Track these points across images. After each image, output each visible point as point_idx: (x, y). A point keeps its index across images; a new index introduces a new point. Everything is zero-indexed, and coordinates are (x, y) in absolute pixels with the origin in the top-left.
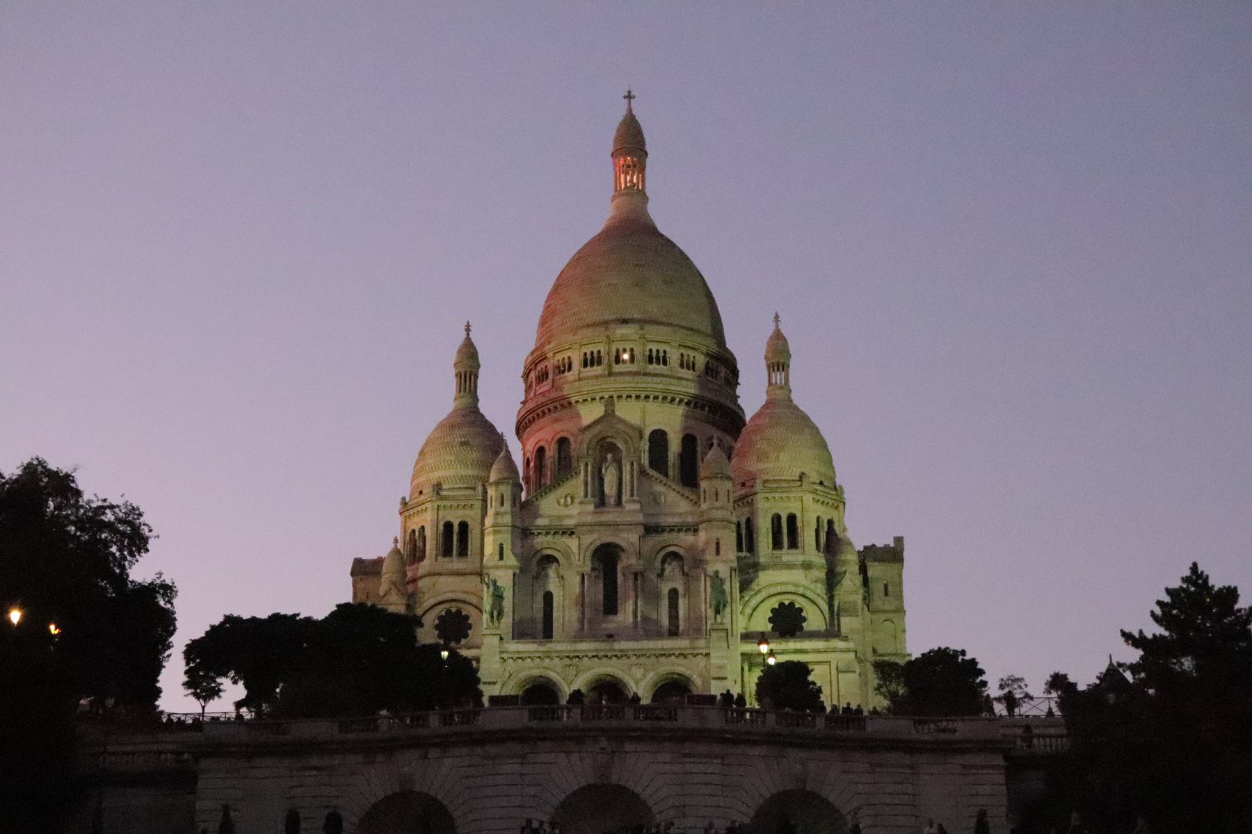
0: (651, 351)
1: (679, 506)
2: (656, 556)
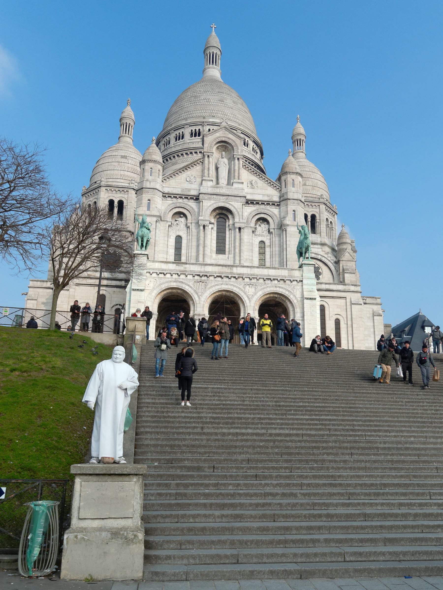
1: (267, 190)
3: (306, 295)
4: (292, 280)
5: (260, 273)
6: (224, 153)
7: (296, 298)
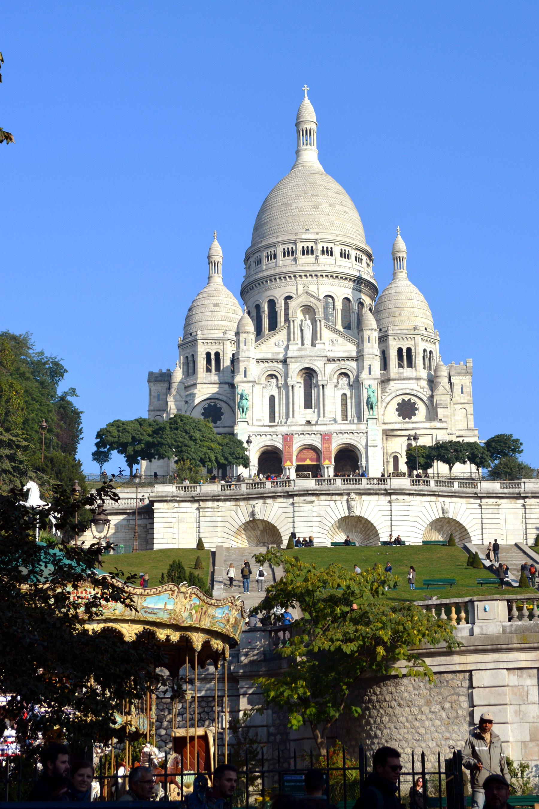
0: (323, 247)
6: (307, 316)
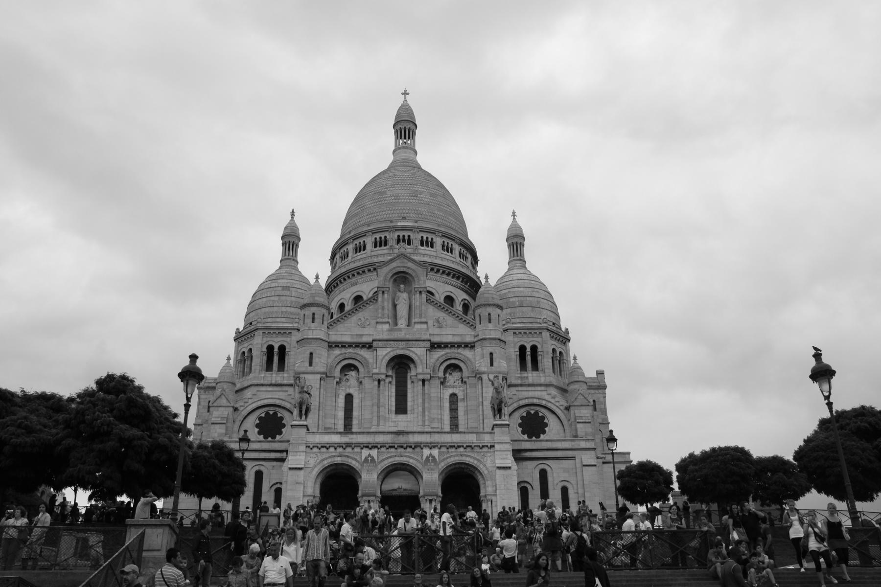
0: (422, 237)
1: (458, 327)
2: (439, 367)
3: (499, 463)
4: (481, 445)
5: (442, 440)
6: (402, 286)
7: (487, 469)
